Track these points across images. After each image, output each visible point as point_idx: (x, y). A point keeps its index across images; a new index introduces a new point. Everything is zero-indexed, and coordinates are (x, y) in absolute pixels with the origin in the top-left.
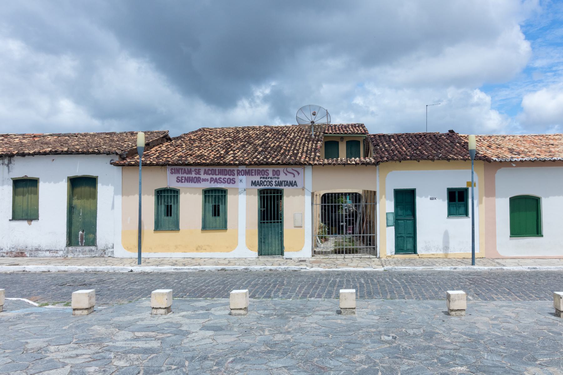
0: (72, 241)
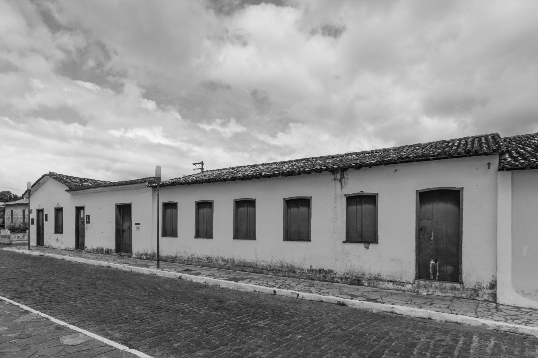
0: (422, 273)
